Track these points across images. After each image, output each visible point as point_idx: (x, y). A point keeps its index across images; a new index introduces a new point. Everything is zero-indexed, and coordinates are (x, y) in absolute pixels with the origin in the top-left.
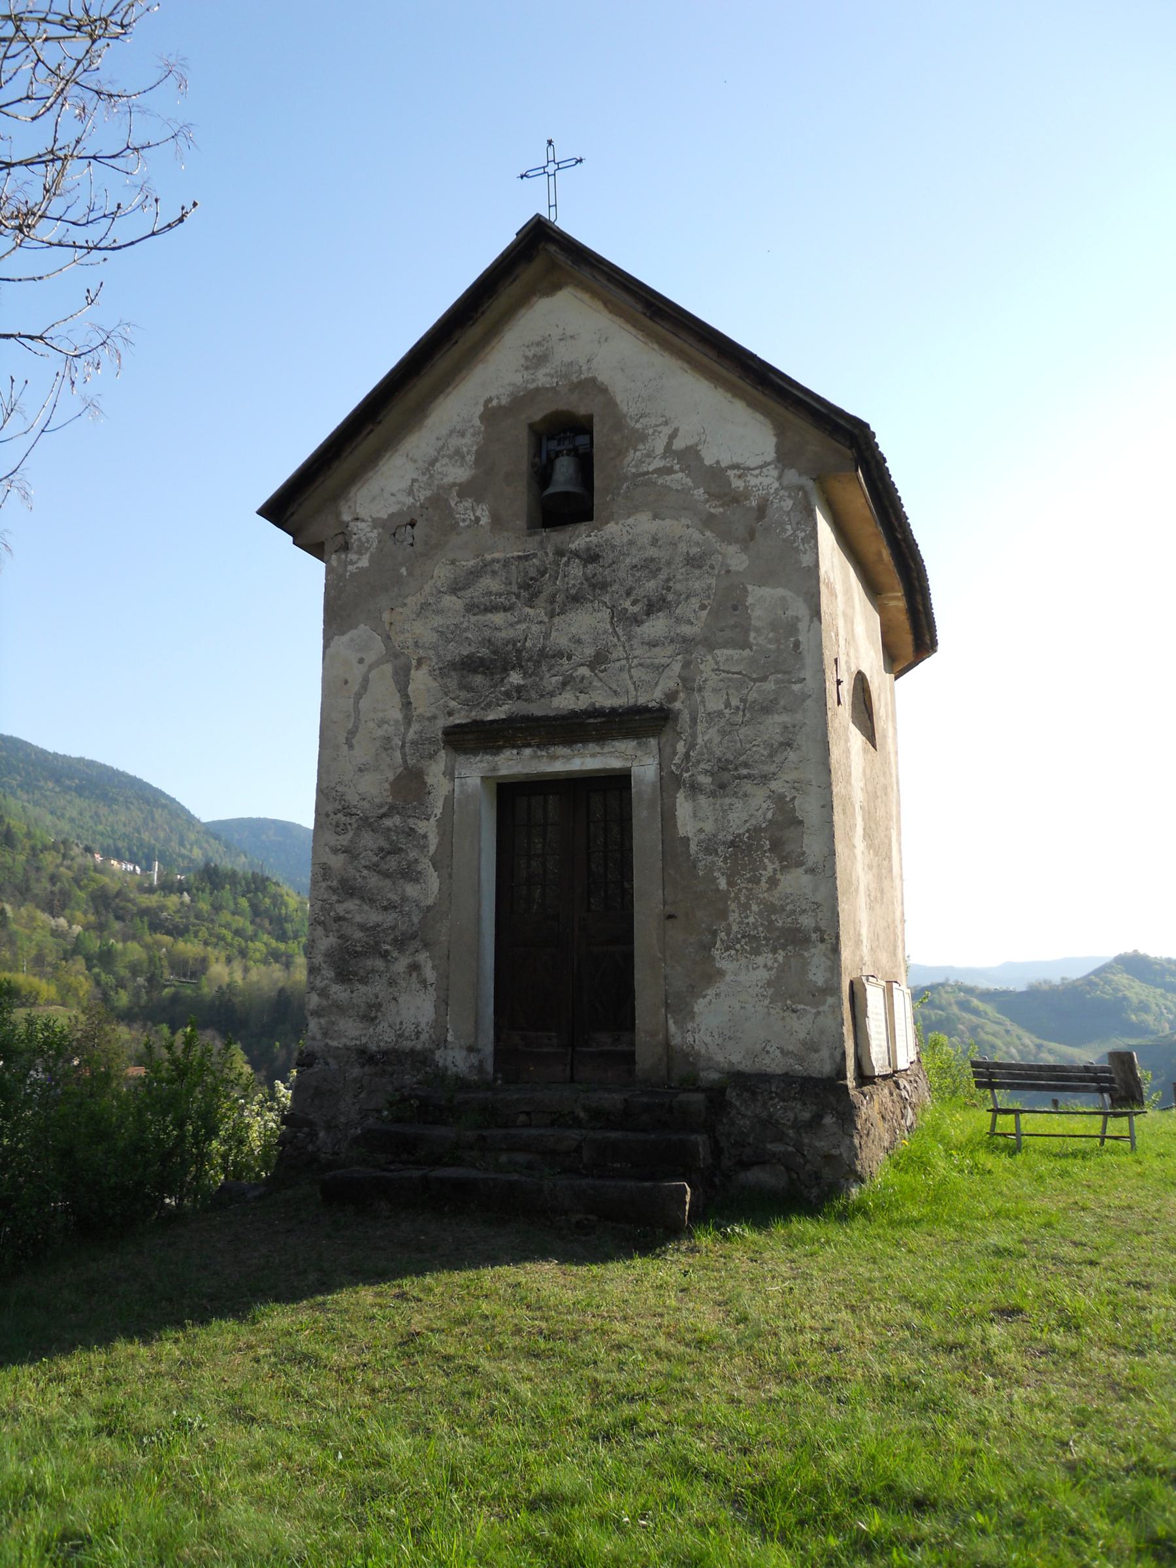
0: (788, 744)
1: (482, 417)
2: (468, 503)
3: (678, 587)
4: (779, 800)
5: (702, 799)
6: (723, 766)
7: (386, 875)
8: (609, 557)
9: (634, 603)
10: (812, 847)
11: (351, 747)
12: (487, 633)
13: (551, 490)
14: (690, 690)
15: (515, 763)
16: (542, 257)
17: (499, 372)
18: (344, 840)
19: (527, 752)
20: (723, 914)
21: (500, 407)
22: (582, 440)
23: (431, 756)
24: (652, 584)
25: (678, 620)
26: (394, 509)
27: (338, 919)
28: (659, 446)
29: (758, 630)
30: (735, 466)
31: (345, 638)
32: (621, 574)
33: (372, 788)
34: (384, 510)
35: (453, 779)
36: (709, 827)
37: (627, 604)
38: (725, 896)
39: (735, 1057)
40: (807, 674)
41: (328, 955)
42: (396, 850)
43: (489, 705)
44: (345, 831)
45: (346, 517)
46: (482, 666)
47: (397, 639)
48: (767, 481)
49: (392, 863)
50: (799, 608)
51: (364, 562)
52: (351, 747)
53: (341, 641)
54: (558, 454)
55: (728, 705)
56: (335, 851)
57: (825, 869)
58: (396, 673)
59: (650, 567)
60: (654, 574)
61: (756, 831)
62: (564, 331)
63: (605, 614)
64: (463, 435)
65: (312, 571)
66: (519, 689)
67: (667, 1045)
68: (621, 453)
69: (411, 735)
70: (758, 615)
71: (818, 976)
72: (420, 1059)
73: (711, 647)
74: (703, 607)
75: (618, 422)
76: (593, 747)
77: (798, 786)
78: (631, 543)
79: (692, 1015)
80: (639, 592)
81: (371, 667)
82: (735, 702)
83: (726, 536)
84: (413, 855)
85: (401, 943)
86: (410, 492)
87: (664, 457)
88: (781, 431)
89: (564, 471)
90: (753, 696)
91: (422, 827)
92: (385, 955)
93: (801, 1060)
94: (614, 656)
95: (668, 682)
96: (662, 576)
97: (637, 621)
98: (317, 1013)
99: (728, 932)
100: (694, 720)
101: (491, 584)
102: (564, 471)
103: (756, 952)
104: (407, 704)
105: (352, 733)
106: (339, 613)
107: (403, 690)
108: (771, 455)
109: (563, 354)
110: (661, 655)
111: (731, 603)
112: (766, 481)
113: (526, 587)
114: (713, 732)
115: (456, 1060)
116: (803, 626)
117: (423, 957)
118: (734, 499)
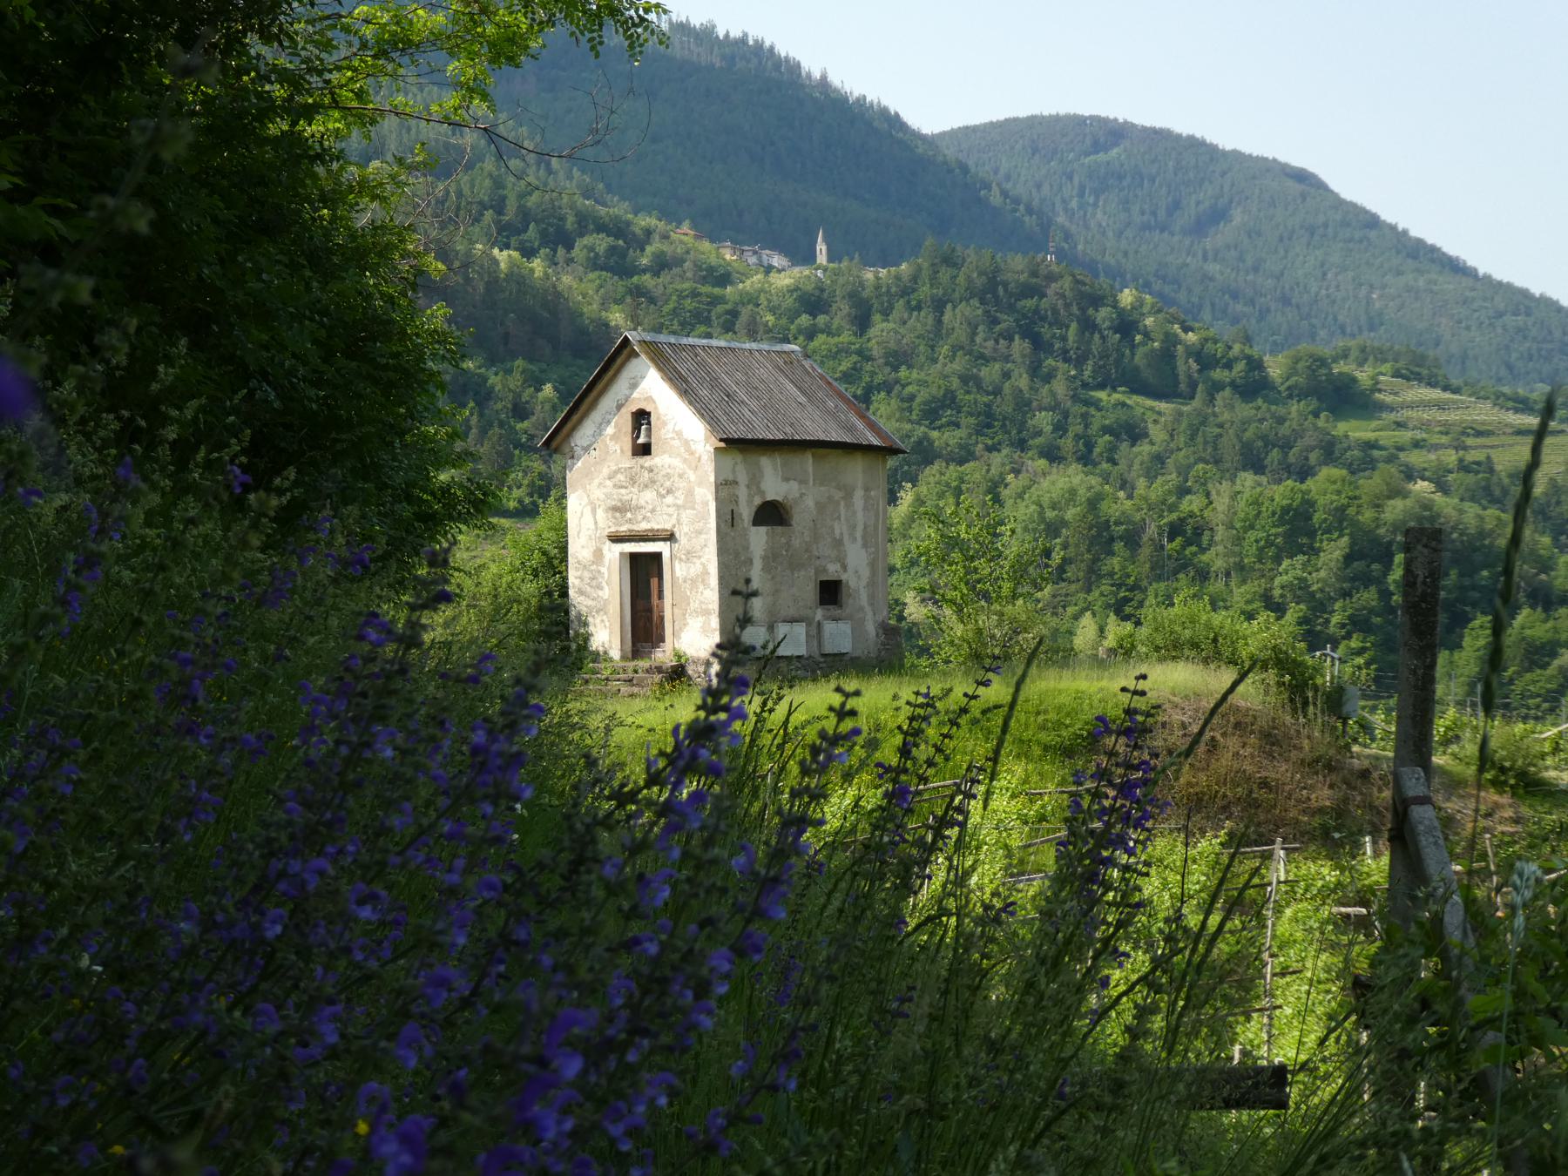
46: (619, 509)
59: (668, 476)
70: (698, 498)
95: (674, 521)
110: (671, 510)
111: (690, 493)
118: (692, 453)
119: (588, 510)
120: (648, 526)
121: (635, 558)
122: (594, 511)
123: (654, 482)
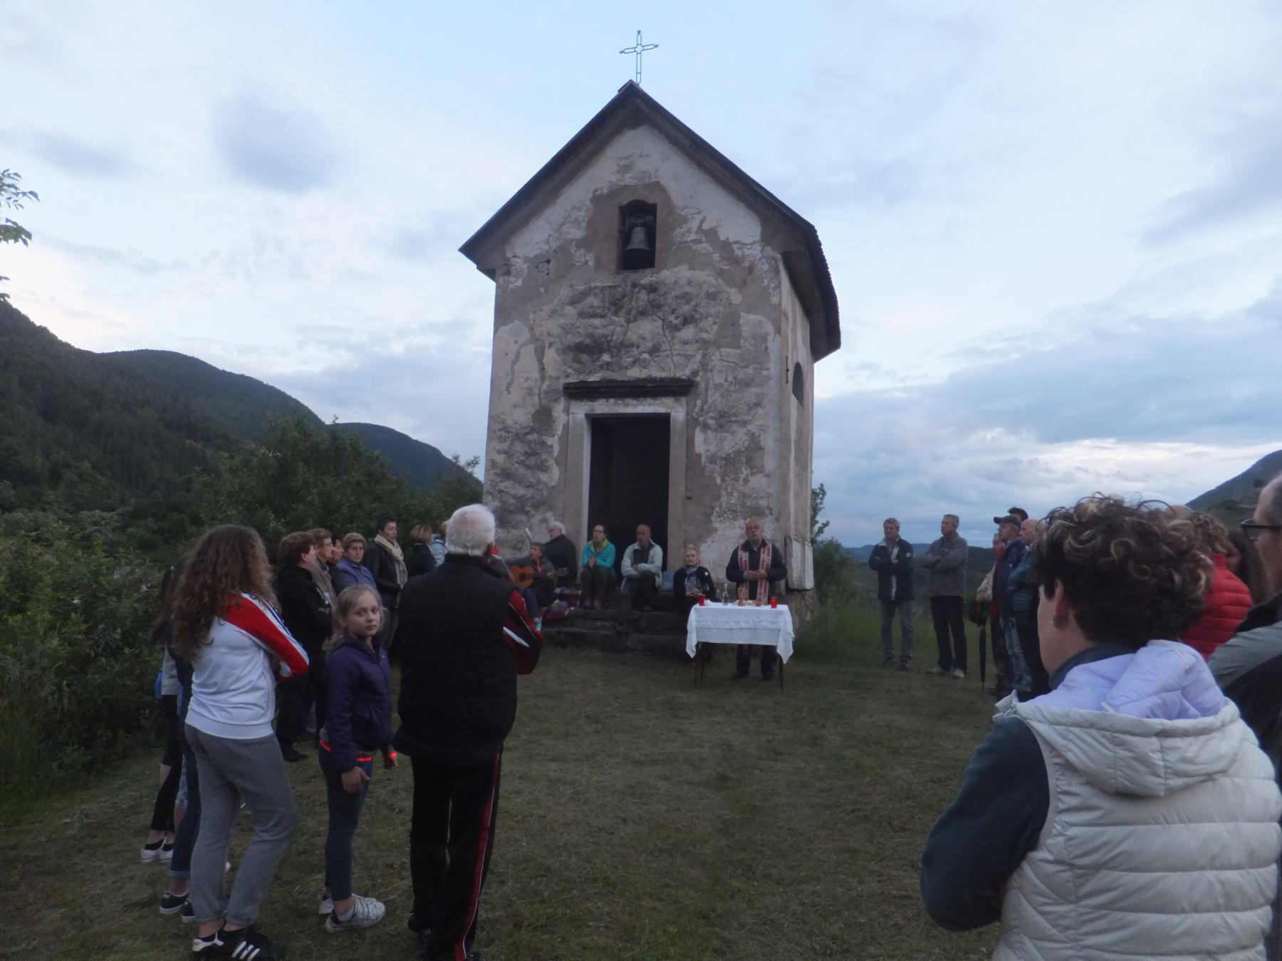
0: (758, 405)
1: (591, 200)
3: (701, 310)
4: (752, 435)
5: (709, 433)
6: (722, 415)
7: (528, 467)
11: (509, 392)
13: (632, 246)
14: (705, 370)
15: (603, 407)
16: (631, 109)
17: (603, 174)
18: (505, 446)
19: (612, 401)
20: (718, 497)
21: (602, 195)
22: (649, 218)
23: (556, 400)
25: (701, 330)
26: (537, 252)
27: (500, 491)
28: (694, 225)
29: (745, 339)
31: (506, 328)
32: (670, 300)
33: (521, 417)
34: (532, 252)
35: (568, 414)
36: (713, 448)
37: (672, 318)
42: (534, 454)
43: (590, 373)
44: (505, 441)
45: (509, 255)
46: (588, 349)
47: (537, 331)
49: (532, 461)
51: (519, 283)
52: (509, 392)
53: (504, 329)
54: (635, 225)
55: (726, 380)
56: (499, 452)
58: (536, 350)
59: (686, 297)
60: (688, 303)
61: (738, 452)
62: (640, 156)
63: (660, 323)
64: (579, 209)
65: (488, 287)
66: (608, 364)
68: (673, 229)
69: (544, 387)
70: (746, 330)
73: (719, 347)
74: (715, 323)
75: (671, 210)
76: (649, 400)
77: (763, 429)
78: (676, 283)
80: (680, 312)
81: (522, 347)
82: (730, 379)
83: (731, 283)
84: (544, 457)
85: (537, 506)
86: (548, 242)
87: (697, 233)
88: (765, 222)
90: (740, 376)
91: (550, 441)
92: (527, 513)
94: (663, 348)
95: (694, 365)
96: (693, 303)
97: (677, 328)
99: (720, 507)
100: (707, 389)
101: (593, 301)
103: (735, 519)
104: (542, 369)
105: (510, 384)
106: (503, 313)
108: (757, 237)
109: (641, 166)
110: (690, 349)
111: (731, 322)
112: (754, 252)
114: (717, 395)
117: (549, 515)
118: (736, 261)
119: (528, 355)
120: (644, 374)
121: (597, 423)
122: (540, 353)
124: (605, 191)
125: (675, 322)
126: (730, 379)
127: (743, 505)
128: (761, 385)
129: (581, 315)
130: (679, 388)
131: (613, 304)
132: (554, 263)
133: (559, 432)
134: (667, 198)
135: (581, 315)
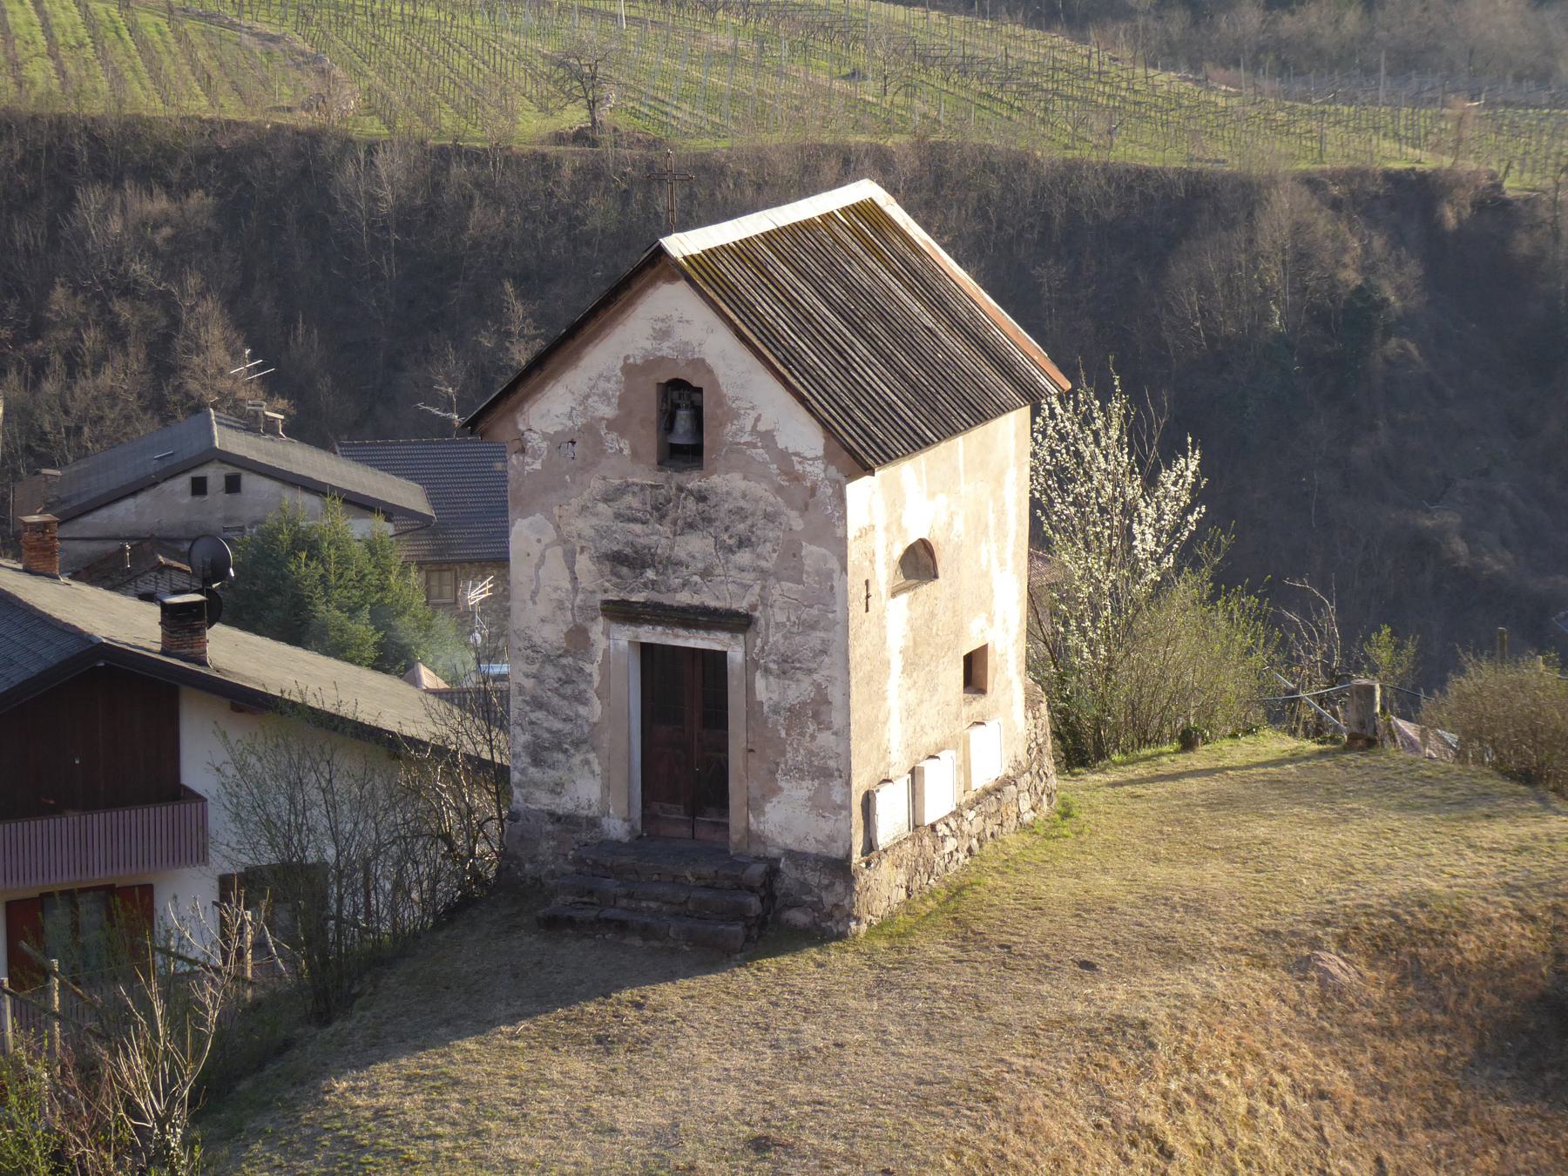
0: (824, 652)
1: (622, 369)
2: (614, 435)
4: (818, 686)
6: (785, 660)
7: (564, 697)
8: (713, 500)
9: (730, 537)
10: (837, 720)
11: (535, 603)
12: (630, 538)
18: (534, 669)
19: (659, 629)
20: (783, 753)
24: (741, 526)
25: (759, 556)
26: (559, 428)
27: (532, 723)
28: (748, 424)
30: (797, 454)
36: (775, 697)
37: (725, 537)
38: (784, 742)
39: (789, 841)
40: (837, 608)
41: (526, 747)
43: (632, 590)
44: (533, 662)
45: (522, 427)
46: (627, 561)
47: (565, 530)
48: (816, 471)
49: (568, 690)
50: (834, 564)
51: (538, 466)
52: (535, 603)
54: (678, 407)
56: (527, 676)
57: (844, 734)
58: (565, 554)
59: (740, 514)
61: (804, 704)
66: (653, 582)
67: (748, 829)
68: (722, 425)
69: (578, 601)
70: (809, 564)
71: (837, 798)
72: (593, 823)
73: (779, 580)
75: (720, 400)
78: (728, 493)
79: (764, 813)
82: (793, 618)
83: (790, 504)
84: (583, 686)
85: (577, 744)
89: (683, 416)
90: (804, 616)
91: (588, 668)
92: (566, 751)
93: (826, 846)
96: (749, 522)
97: (731, 550)
98: (520, 785)
102: (683, 418)
103: (802, 779)
104: (574, 579)
105: (534, 594)
107: (573, 572)
108: (820, 452)
109: (682, 334)
110: (748, 578)
111: (792, 552)
112: (817, 471)
113: (656, 508)
114: (779, 636)
115: (616, 828)
116: (836, 576)
117: (592, 756)
118: (796, 478)
119: (555, 558)
120: (696, 600)
123: (709, 521)
124: (639, 362)
125: (731, 542)
126: (793, 618)
127: (811, 764)
128: (826, 630)
129: (618, 516)
130: (738, 622)
131: (656, 508)
132: (578, 443)
133: (599, 659)
134: (715, 383)
135: (618, 516)
